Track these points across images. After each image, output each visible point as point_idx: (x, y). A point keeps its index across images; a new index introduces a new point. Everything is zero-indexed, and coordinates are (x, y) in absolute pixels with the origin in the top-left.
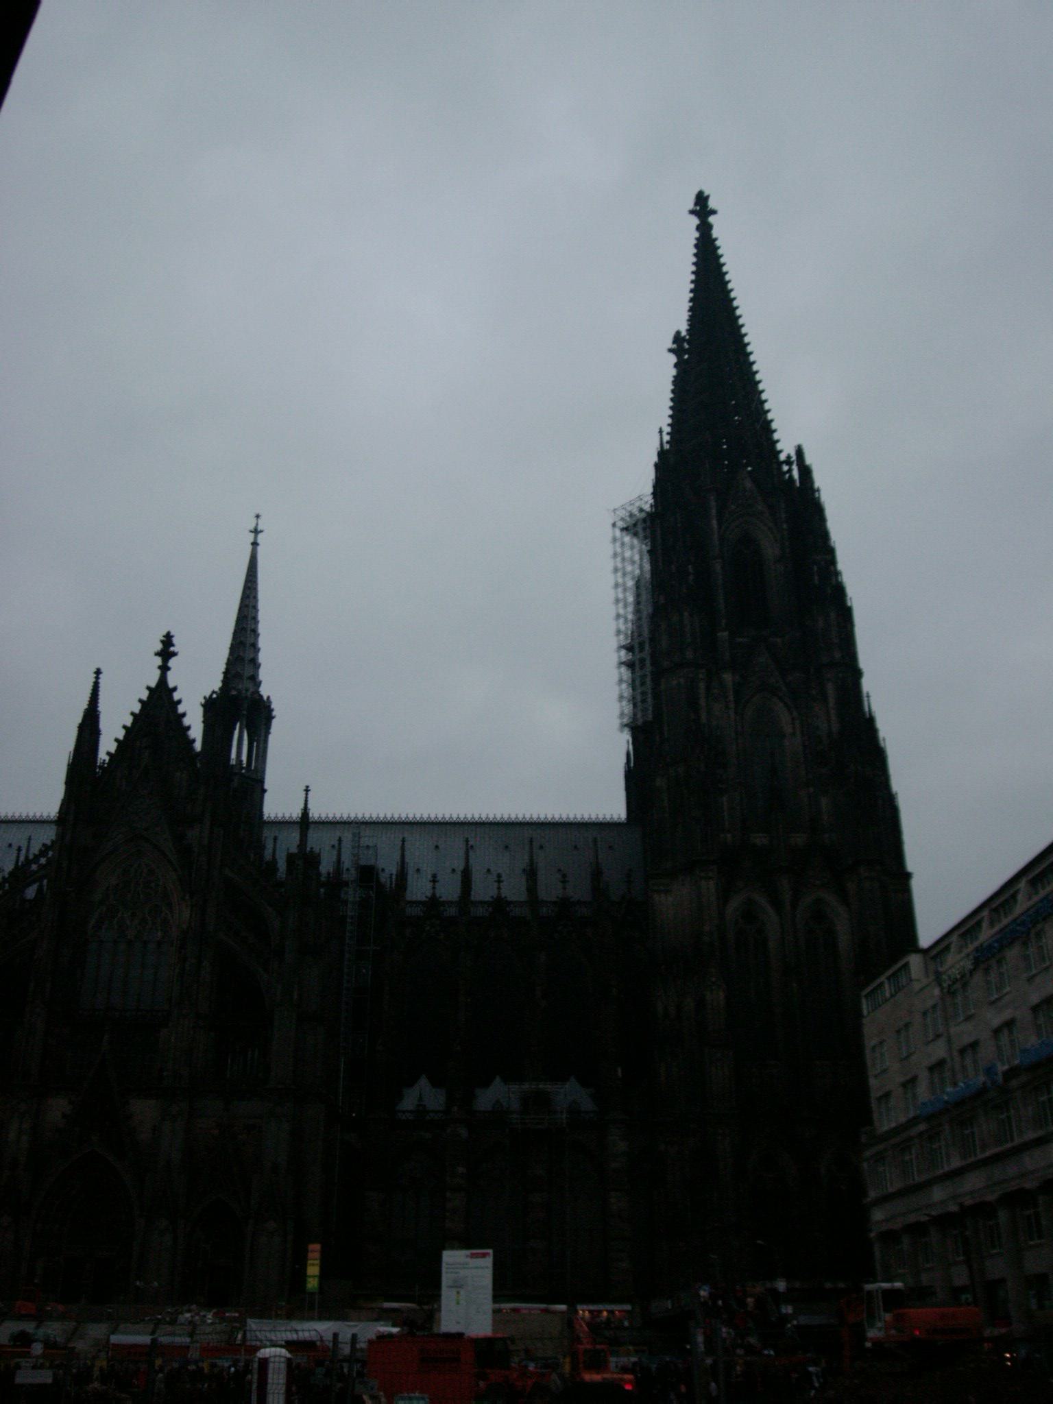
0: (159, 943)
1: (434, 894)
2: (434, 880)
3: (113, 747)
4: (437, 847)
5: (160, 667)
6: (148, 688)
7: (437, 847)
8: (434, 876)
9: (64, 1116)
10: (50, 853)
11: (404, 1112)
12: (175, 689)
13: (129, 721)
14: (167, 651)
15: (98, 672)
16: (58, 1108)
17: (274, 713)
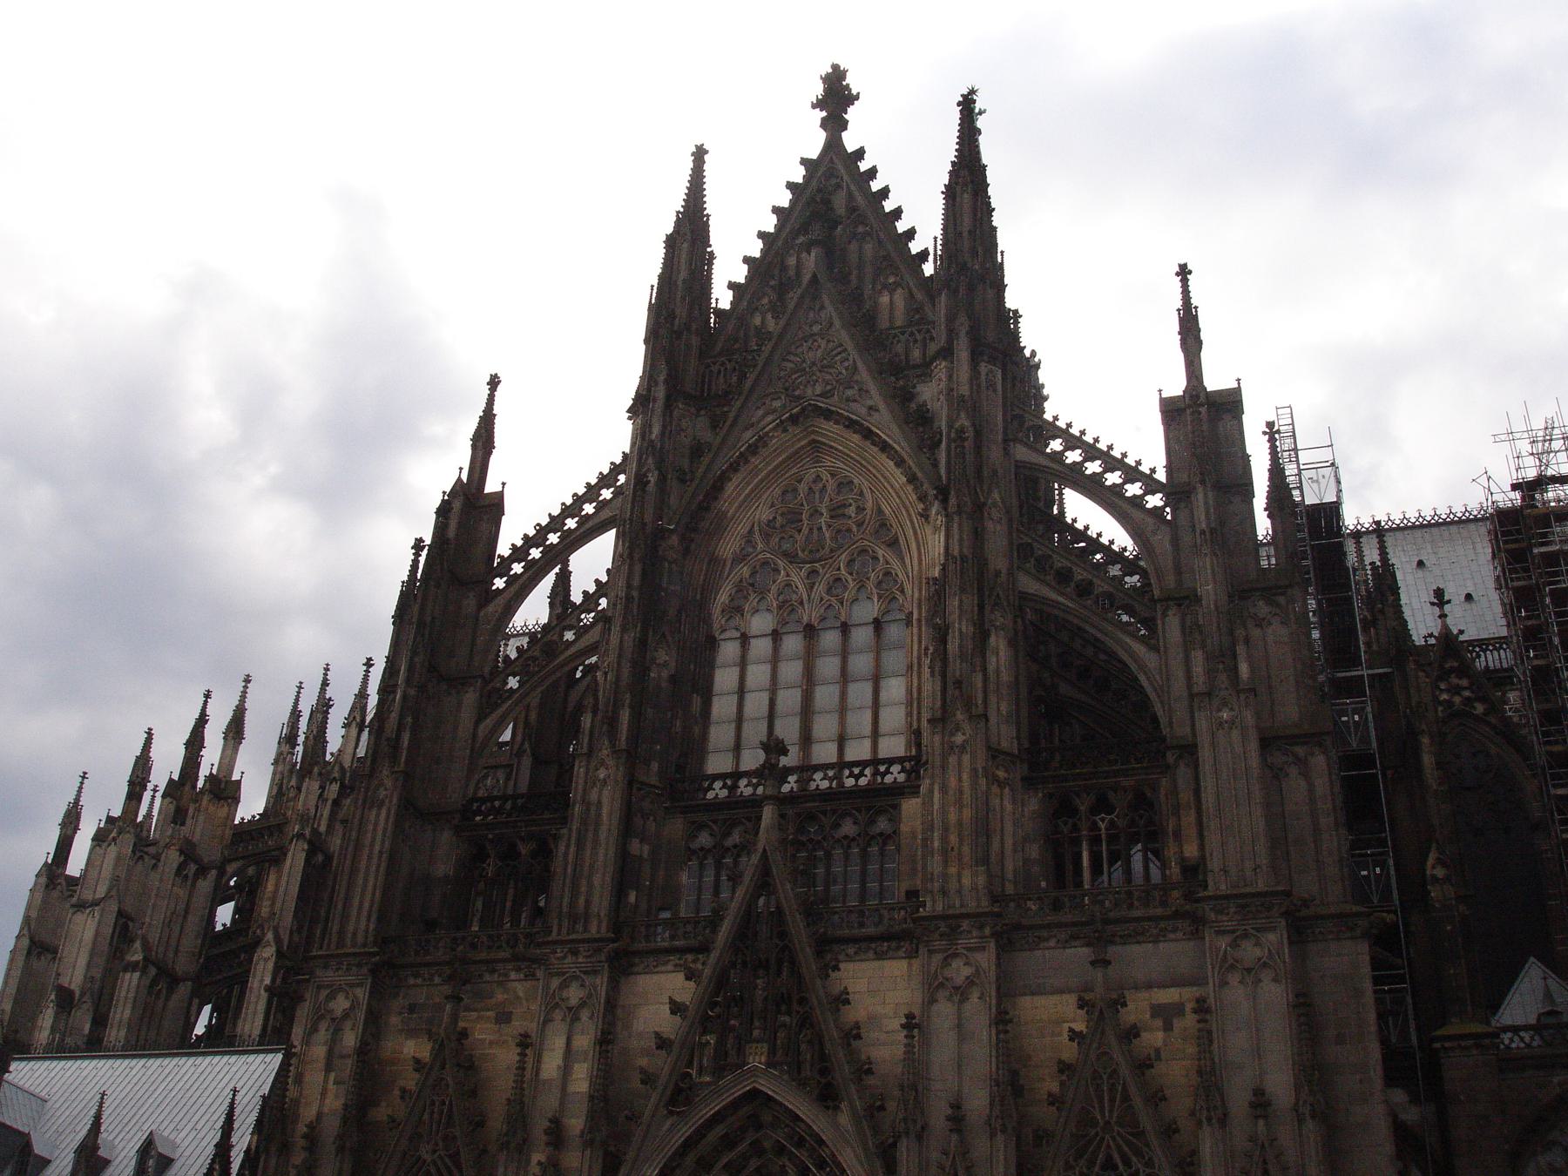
0: (878, 625)
1: (1445, 627)
2: (1440, 598)
3: (740, 274)
4: (1421, 564)
5: (824, 124)
6: (804, 162)
7: (1421, 564)
8: (1439, 593)
9: (676, 1008)
10: (622, 478)
11: (1515, 1029)
12: (860, 154)
13: (770, 224)
14: (836, 98)
15: (700, 154)
16: (660, 998)
17: (1045, 392)
